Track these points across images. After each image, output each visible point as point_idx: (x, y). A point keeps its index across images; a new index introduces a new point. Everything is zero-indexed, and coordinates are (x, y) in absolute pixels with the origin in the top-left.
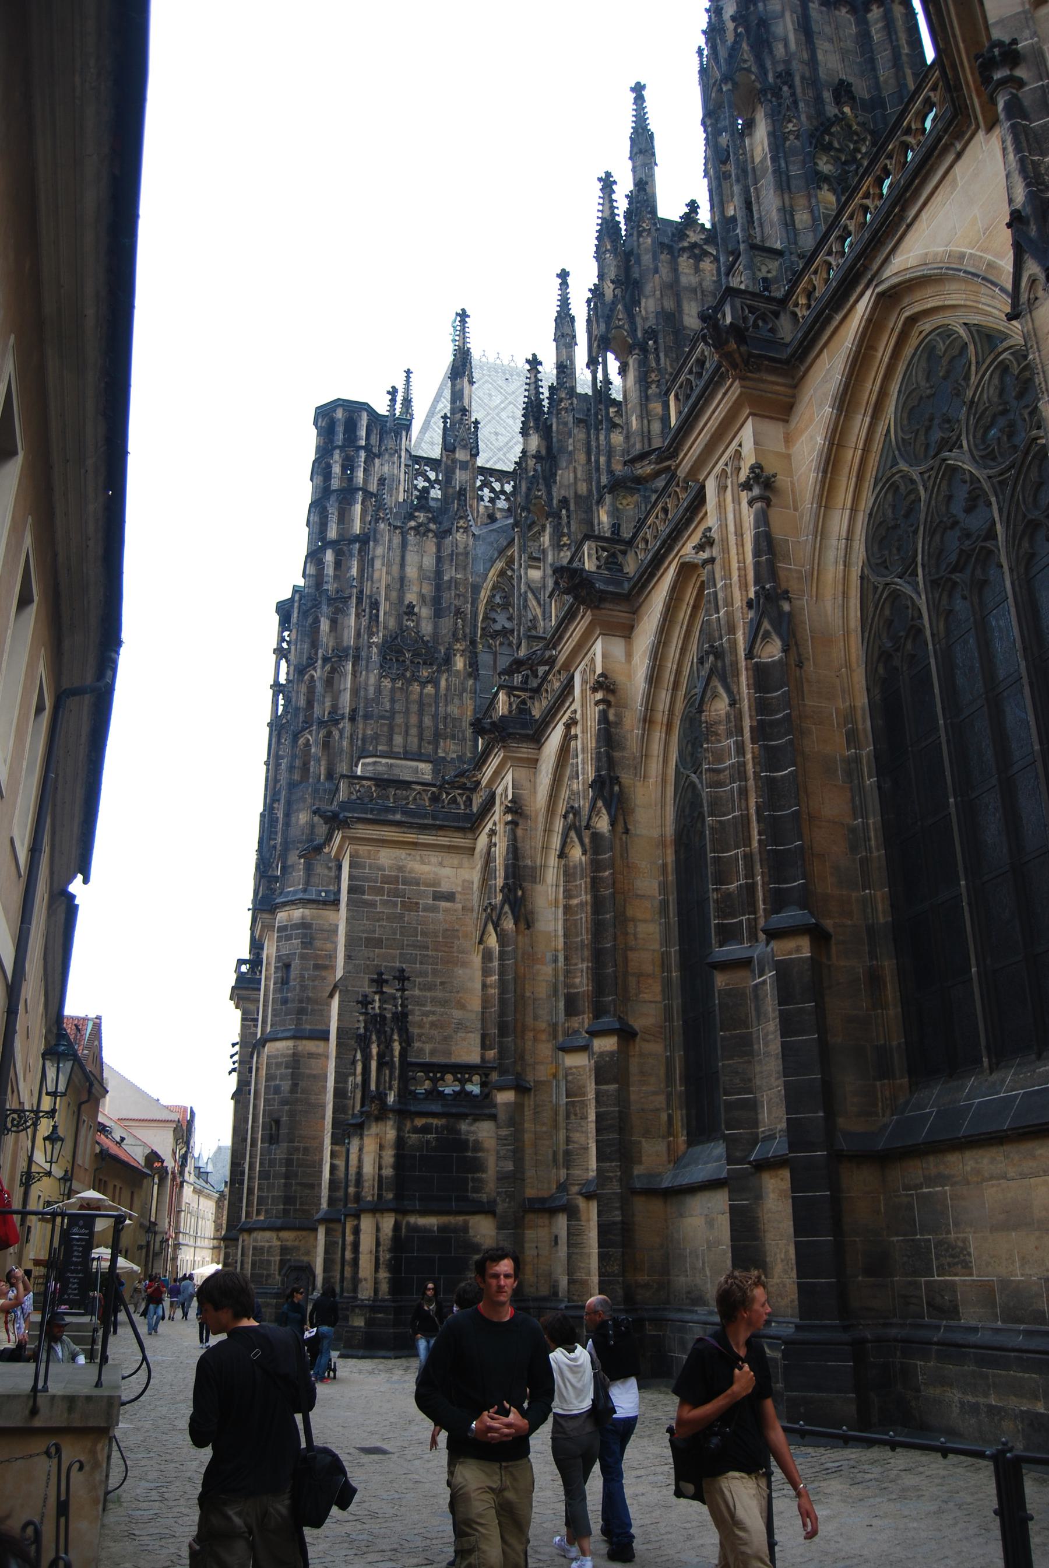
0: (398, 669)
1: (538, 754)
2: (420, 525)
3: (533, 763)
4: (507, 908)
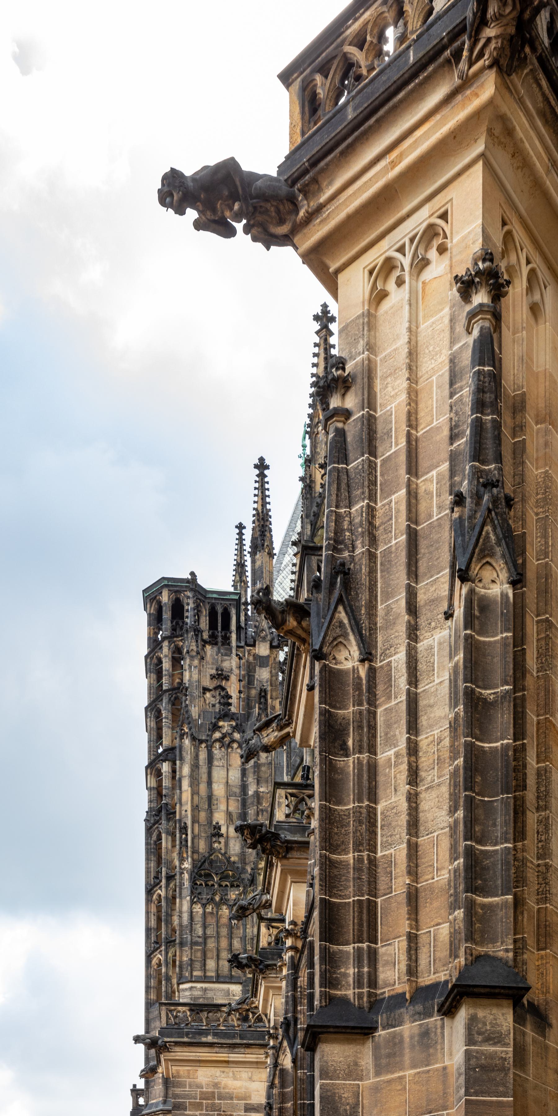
0: (207, 894)
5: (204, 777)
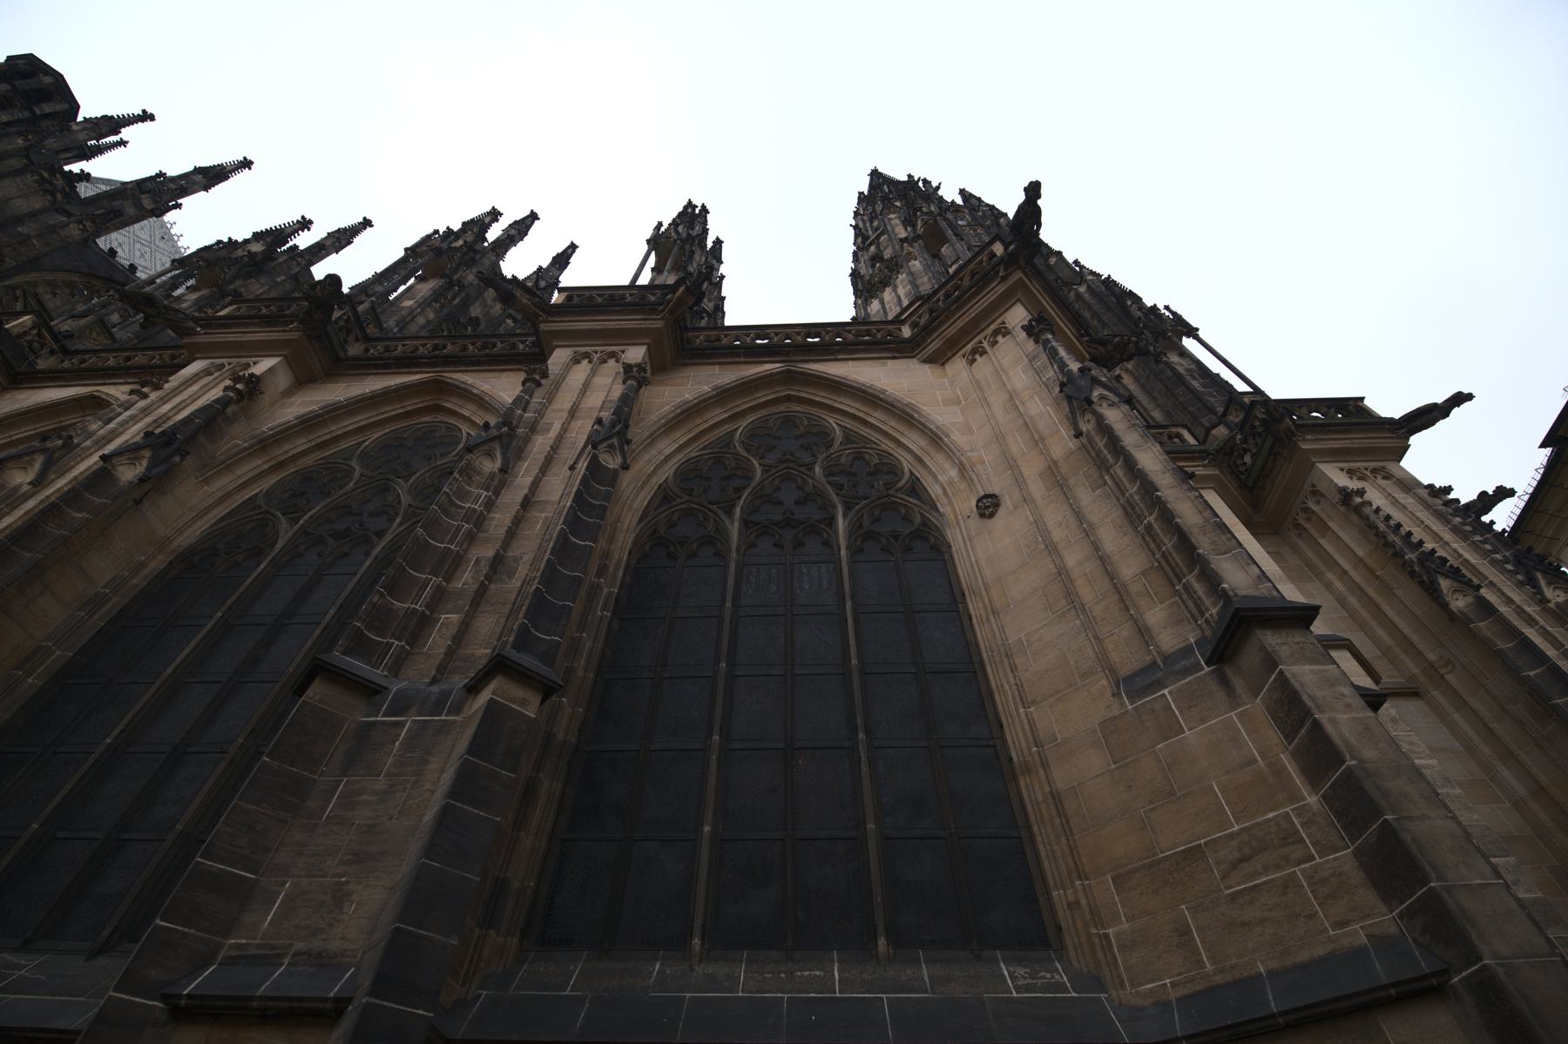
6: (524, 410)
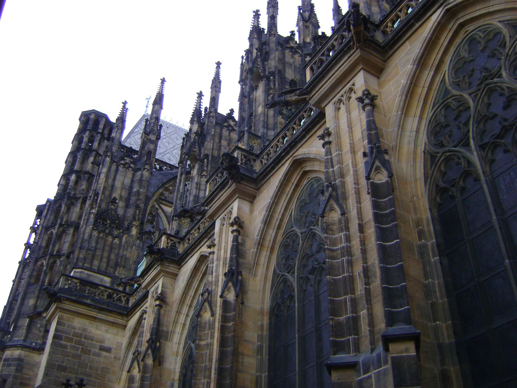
0: (102, 228)
1: (178, 272)
2: (126, 163)
3: (175, 276)
4: (150, 352)
5: (112, 176)
6: (333, 167)
